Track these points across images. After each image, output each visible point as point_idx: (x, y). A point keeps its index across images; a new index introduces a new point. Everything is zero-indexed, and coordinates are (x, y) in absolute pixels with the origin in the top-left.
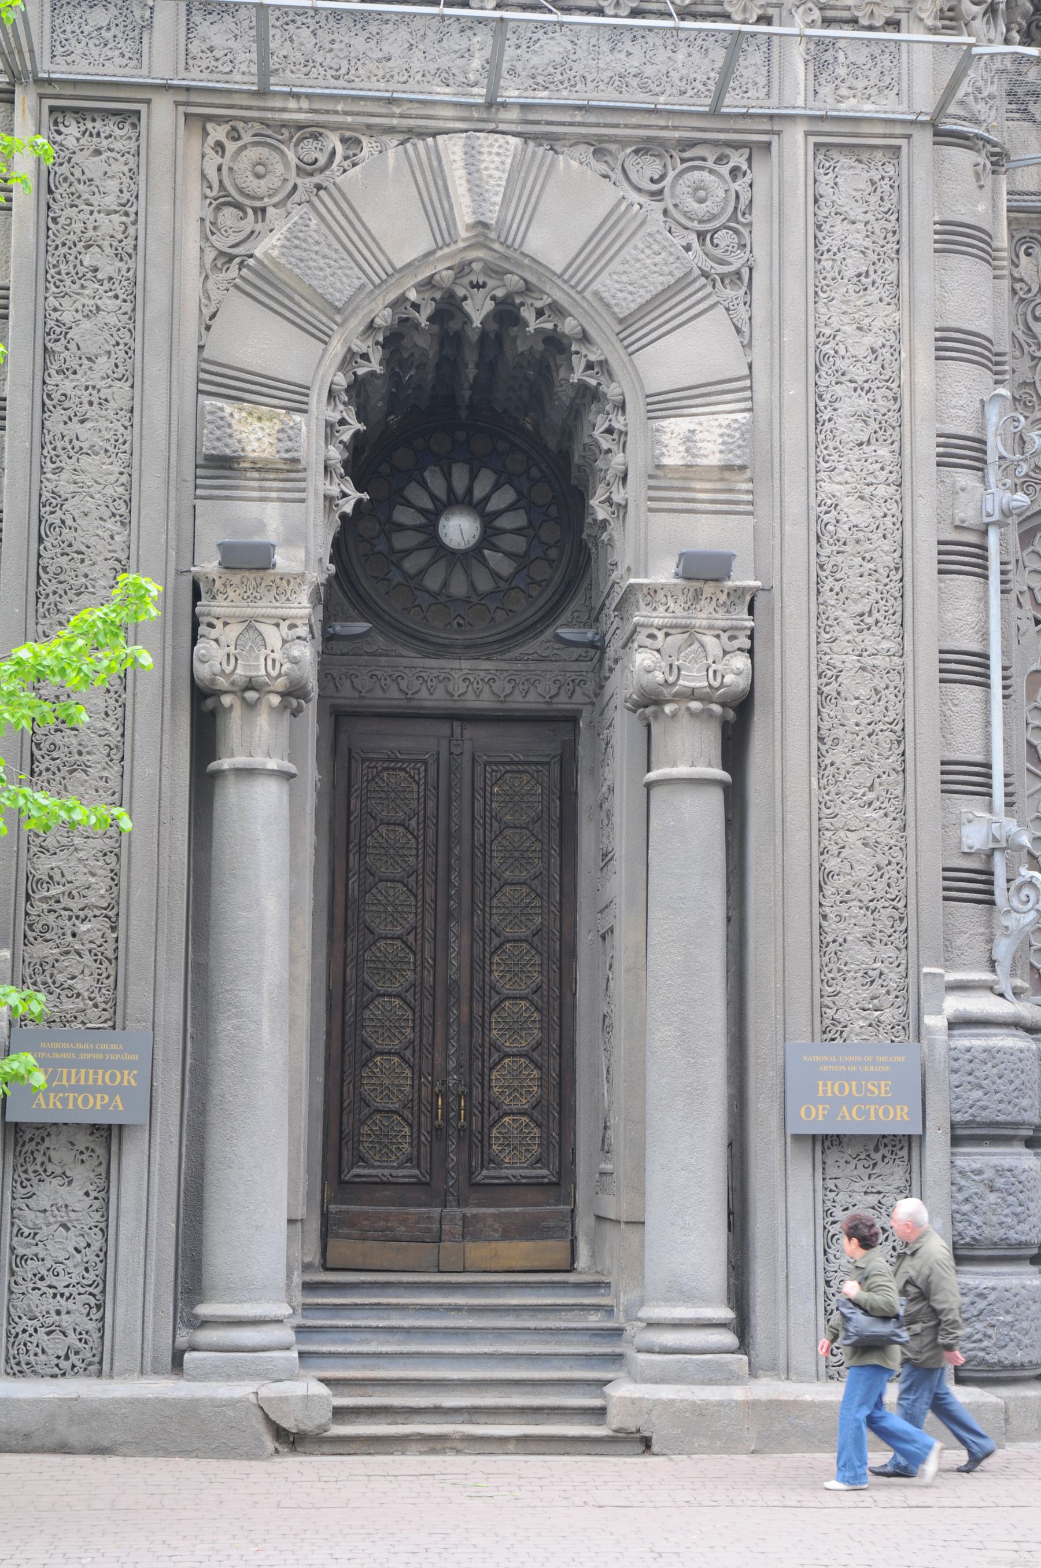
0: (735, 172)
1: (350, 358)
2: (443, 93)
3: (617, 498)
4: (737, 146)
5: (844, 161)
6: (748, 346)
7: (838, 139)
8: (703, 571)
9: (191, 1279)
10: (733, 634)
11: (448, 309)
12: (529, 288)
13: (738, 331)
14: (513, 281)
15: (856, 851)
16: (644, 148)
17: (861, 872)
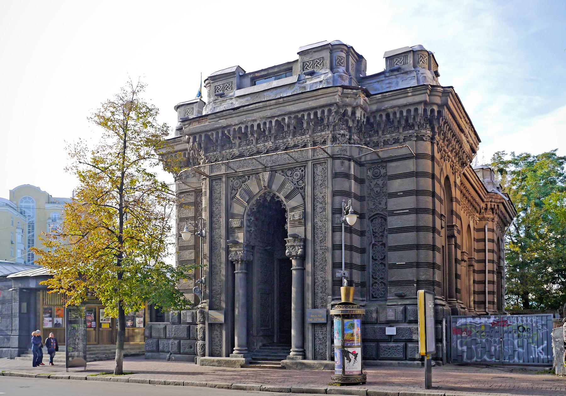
0: (302, 171)
1: (251, 209)
4: (302, 166)
5: (318, 166)
6: (304, 199)
7: (316, 163)
8: (295, 237)
11: (265, 200)
12: (275, 195)
13: (303, 196)
15: (320, 279)
16: (289, 169)
17: (320, 282)
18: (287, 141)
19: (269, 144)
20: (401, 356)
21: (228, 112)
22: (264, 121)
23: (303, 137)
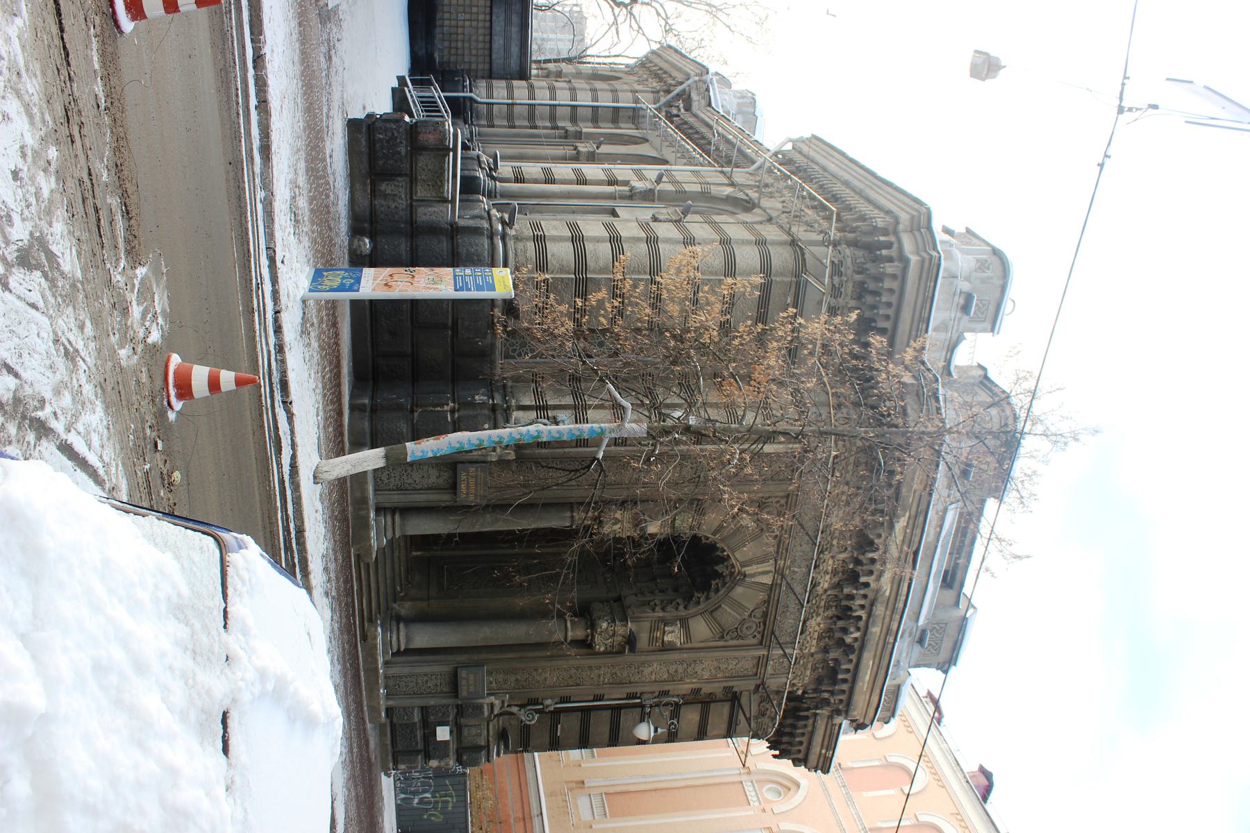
2: (788, 563)
3: (657, 608)
5: (755, 662)
7: (761, 662)
9: (406, 511)
10: (613, 647)
14: (728, 579)
15: (544, 675)
16: (765, 614)
18: (818, 615)
19: (825, 582)
20: (400, 747)
21: (917, 540)
22: (871, 595)
23: (814, 642)
